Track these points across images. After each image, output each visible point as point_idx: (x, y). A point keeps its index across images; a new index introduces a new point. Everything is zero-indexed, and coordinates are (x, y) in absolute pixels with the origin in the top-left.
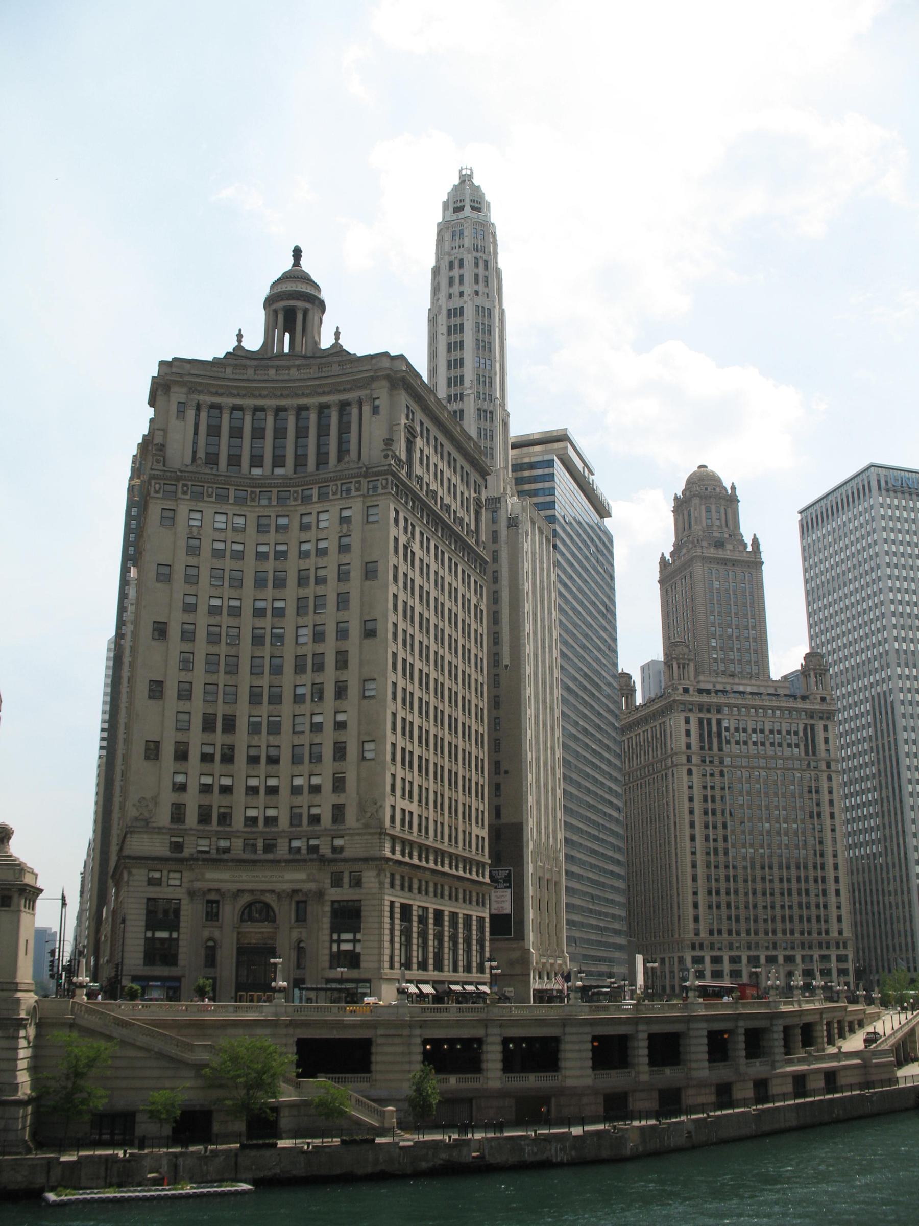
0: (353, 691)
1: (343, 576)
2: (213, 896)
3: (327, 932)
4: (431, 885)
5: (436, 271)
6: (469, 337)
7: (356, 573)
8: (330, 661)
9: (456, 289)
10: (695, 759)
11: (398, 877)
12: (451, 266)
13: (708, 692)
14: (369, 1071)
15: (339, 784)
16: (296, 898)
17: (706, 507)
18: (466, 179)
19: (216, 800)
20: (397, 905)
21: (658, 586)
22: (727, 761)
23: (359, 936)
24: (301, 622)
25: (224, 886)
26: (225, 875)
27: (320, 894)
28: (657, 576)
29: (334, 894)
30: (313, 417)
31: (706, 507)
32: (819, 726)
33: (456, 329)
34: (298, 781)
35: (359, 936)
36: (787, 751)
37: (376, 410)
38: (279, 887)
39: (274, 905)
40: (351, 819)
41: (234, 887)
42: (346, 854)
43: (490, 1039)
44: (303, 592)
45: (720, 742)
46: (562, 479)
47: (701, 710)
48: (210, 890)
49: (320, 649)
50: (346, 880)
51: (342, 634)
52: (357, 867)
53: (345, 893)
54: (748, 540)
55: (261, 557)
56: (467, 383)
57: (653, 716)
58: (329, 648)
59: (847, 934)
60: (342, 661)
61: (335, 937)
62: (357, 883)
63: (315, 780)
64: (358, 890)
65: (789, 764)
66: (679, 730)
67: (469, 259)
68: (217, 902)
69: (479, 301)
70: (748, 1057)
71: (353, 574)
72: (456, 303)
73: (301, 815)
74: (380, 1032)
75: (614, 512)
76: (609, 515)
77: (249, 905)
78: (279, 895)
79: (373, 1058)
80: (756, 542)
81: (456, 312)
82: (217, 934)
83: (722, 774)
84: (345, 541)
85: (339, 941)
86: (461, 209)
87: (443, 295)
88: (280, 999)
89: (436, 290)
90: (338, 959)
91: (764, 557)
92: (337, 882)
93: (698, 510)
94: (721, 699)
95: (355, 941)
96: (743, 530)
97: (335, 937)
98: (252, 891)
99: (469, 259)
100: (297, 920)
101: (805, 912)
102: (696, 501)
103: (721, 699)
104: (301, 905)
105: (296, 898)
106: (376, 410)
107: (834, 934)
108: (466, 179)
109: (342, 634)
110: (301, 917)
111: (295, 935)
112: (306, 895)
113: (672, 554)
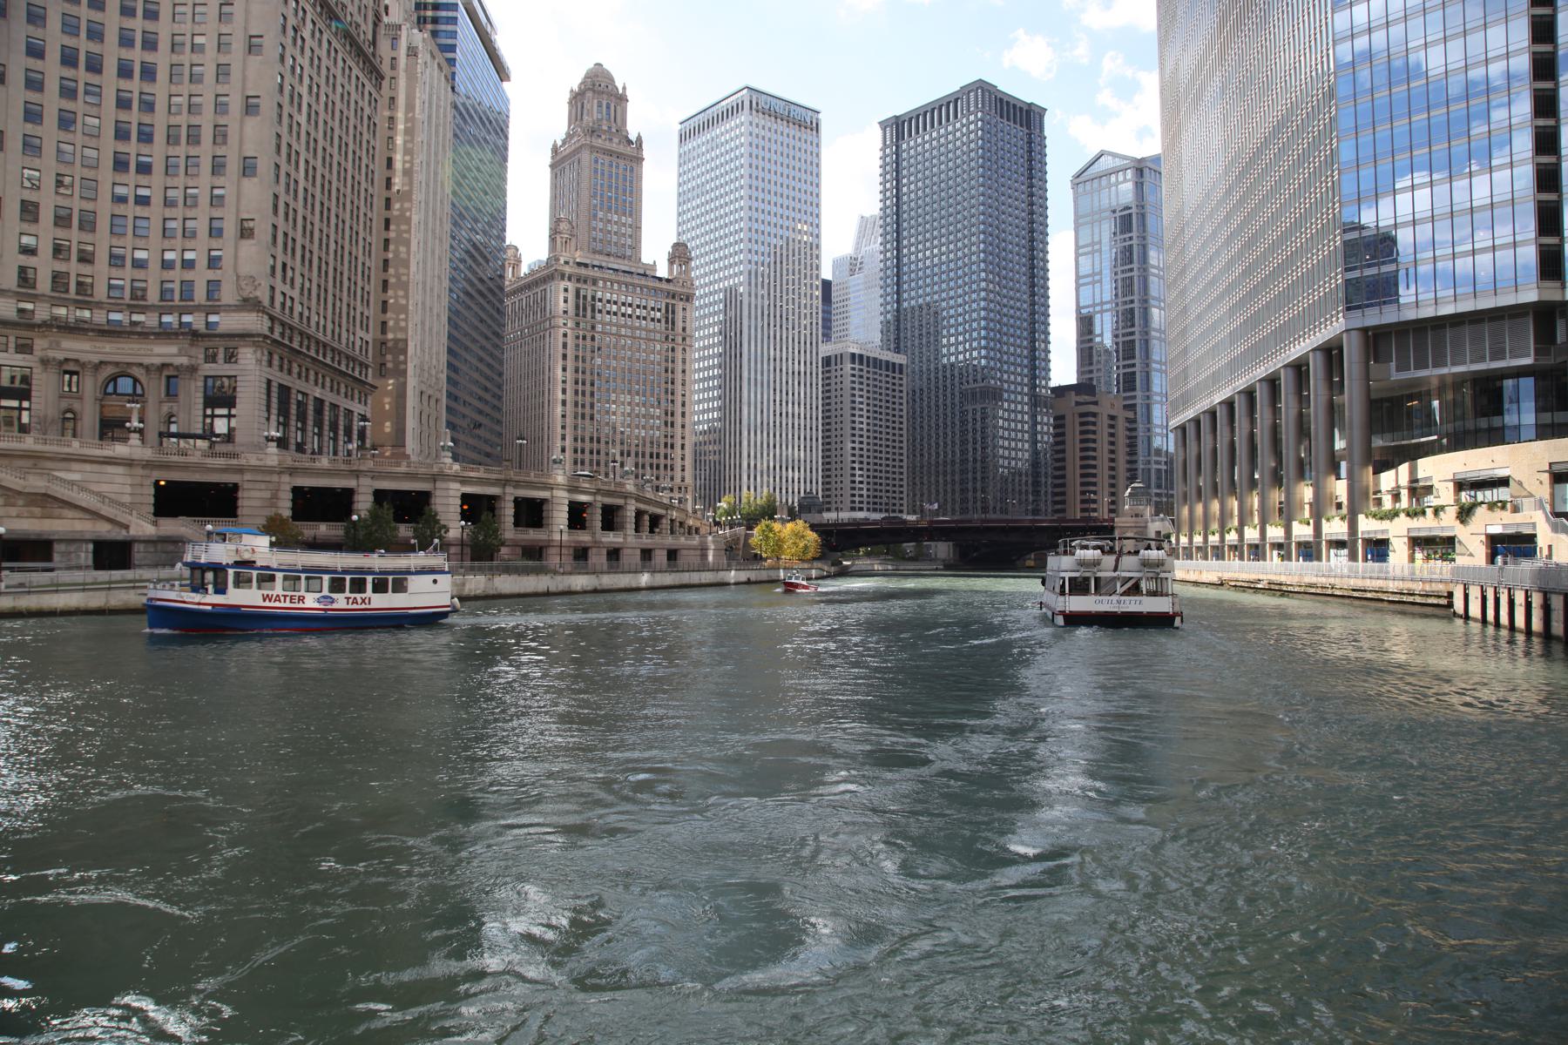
2: (71, 367)
3: (201, 406)
4: (312, 373)
8: (207, 134)
11: (276, 357)
13: (586, 265)
14: (236, 516)
15: (213, 263)
16: (166, 373)
17: (598, 101)
19: (73, 267)
20: (275, 384)
21: (549, 169)
22: (599, 328)
23: (233, 412)
24: (174, 89)
25: (84, 358)
26: (86, 346)
27: (193, 369)
28: (549, 161)
31: (598, 101)
32: (680, 305)
34: (169, 256)
35: (233, 412)
36: (651, 325)
38: (146, 361)
39: (143, 379)
40: (228, 295)
41: (96, 359)
42: (221, 329)
43: (361, 490)
44: (176, 59)
45: (593, 310)
46: (465, 27)
47: (578, 281)
48: (67, 360)
49: (195, 121)
50: (221, 356)
51: (220, 108)
52: (231, 344)
53: (220, 368)
54: (633, 137)
57: (536, 283)
58: (206, 120)
59: (689, 480)
60: (220, 135)
61: (209, 412)
62: (231, 357)
63: (189, 256)
64: (234, 366)
65: (652, 336)
66: (560, 298)
68: (76, 373)
70: (603, 529)
71: (234, 46)
73: (172, 290)
74: (248, 477)
75: (513, 76)
76: (508, 79)
77: (114, 379)
78: (147, 368)
79: (240, 503)
80: (639, 139)
82: (76, 406)
83: (593, 339)
84: (226, 9)
85: (213, 416)
88: (135, 439)
91: (645, 154)
92: (212, 358)
93: (592, 104)
94: (596, 273)
95: (229, 416)
96: (629, 128)
97: (209, 412)
98: (117, 364)
100: (168, 394)
101: (655, 461)
102: (589, 94)
103: (596, 273)
104: (171, 377)
105: (166, 373)
107: (678, 480)
109: (220, 108)
110: (171, 394)
111: (165, 408)
112: (177, 368)
113: (564, 142)
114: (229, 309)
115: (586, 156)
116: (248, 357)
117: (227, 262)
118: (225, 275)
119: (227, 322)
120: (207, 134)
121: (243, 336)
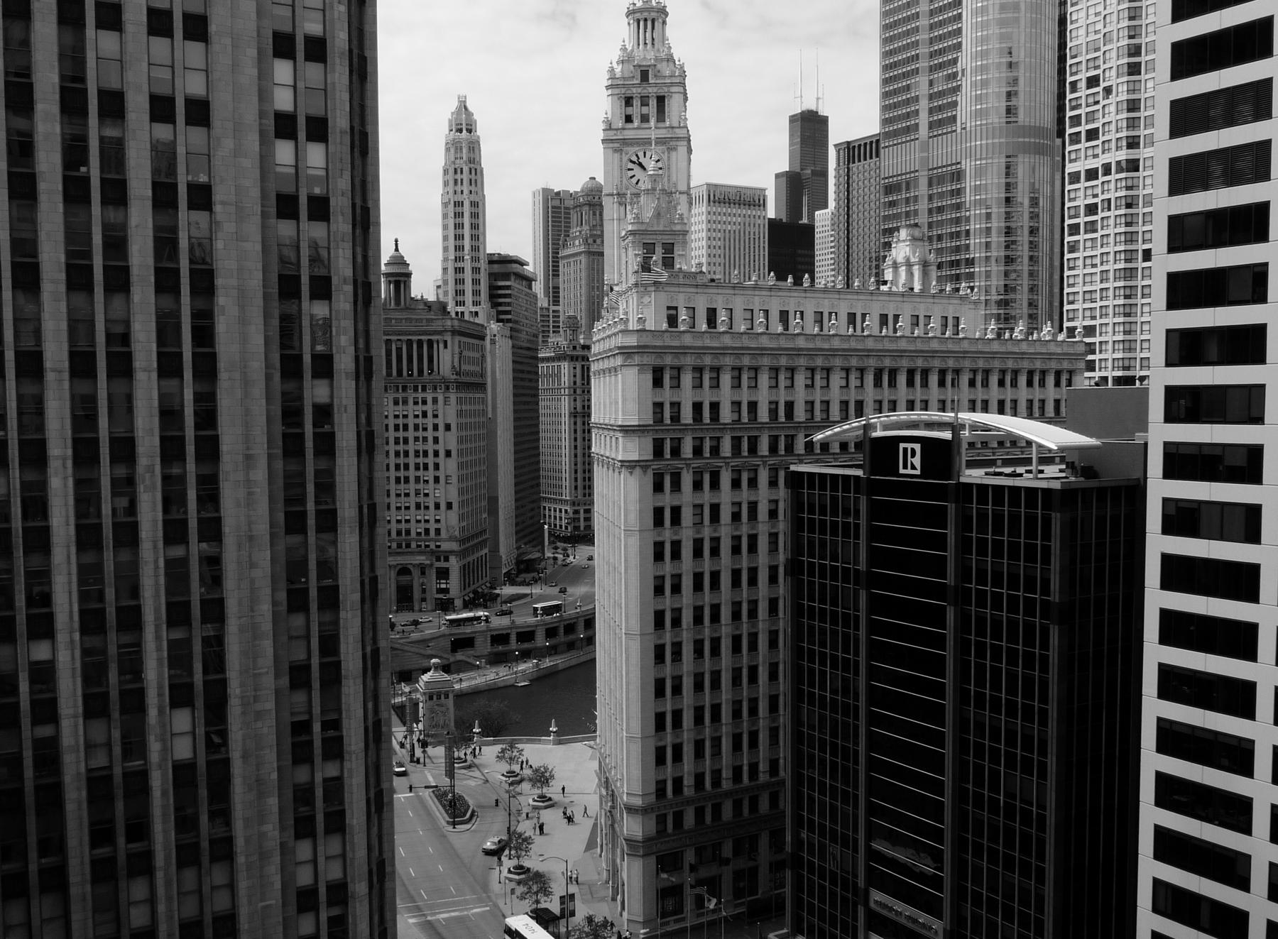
0: (442, 480)
1: (436, 427)
5: (446, 172)
6: (467, 220)
7: (441, 427)
8: (431, 467)
9: (459, 188)
10: (579, 391)
12: (456, 172)
18: (463, 107)
27: (431, 565)
29: (438, 564)
30: (415, 346)
33: (459, 215)
37: (446, 347)
40: (443, 532)
51: (436, 454)
53: (442, 564)
55: (396, 417)
56: (466, 251)
62: (447, 559)
67: (466, 170)
69: (473, 197)
72: (459, 198)
78: (414, 566)
81: (458, 204)
86: (460, 131)
87: (451, 189)
89: (446, 184)
90: (440, 591)
92: (438, 559)
99: (466, 170)
104: (423, 570)
106: (446, 347)
108: (463, 107)
110: (423, 573)
114: (445, 540)
115: (583, 258)
116: (453, 559)
117: (443, 521)
118: (442, 526)
119: (446, 546)
120: (431, 467)
121: (452, 552)
